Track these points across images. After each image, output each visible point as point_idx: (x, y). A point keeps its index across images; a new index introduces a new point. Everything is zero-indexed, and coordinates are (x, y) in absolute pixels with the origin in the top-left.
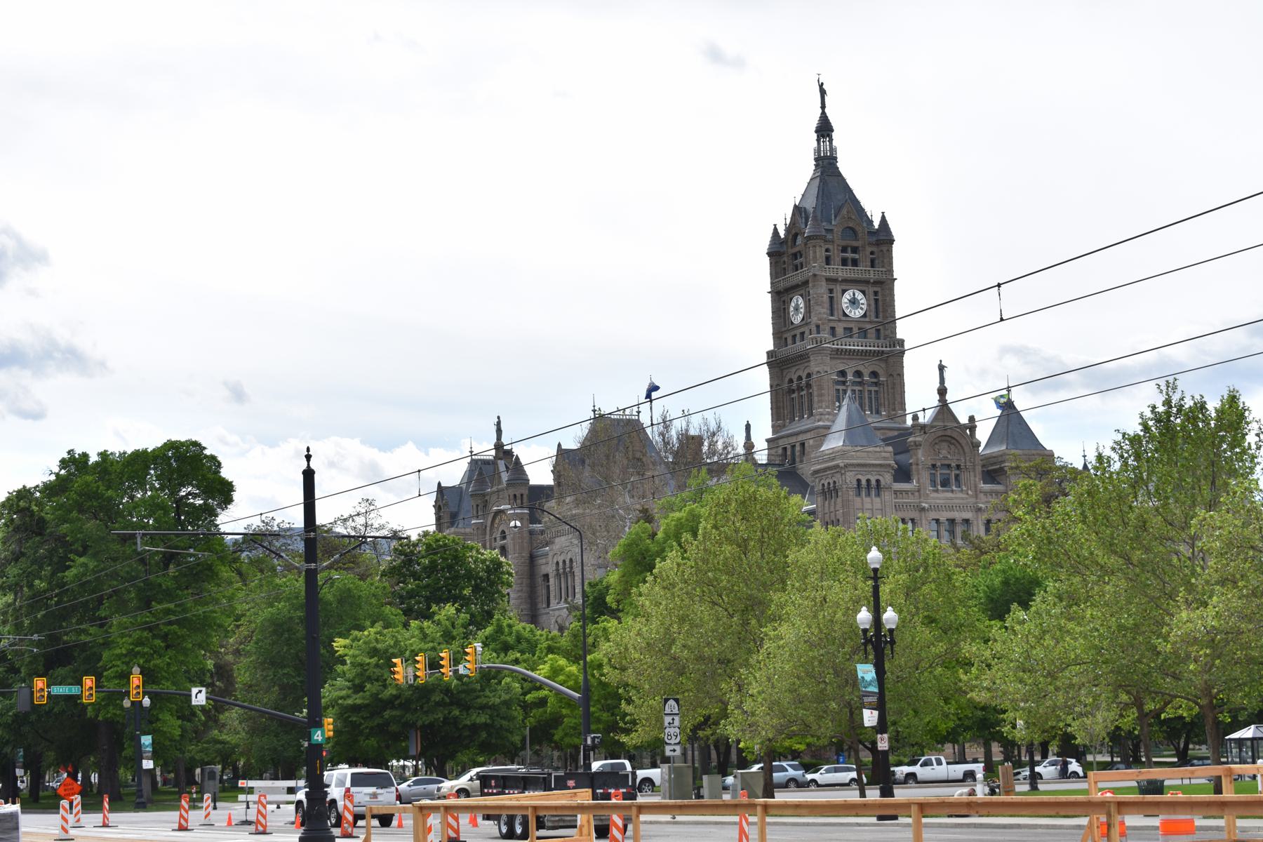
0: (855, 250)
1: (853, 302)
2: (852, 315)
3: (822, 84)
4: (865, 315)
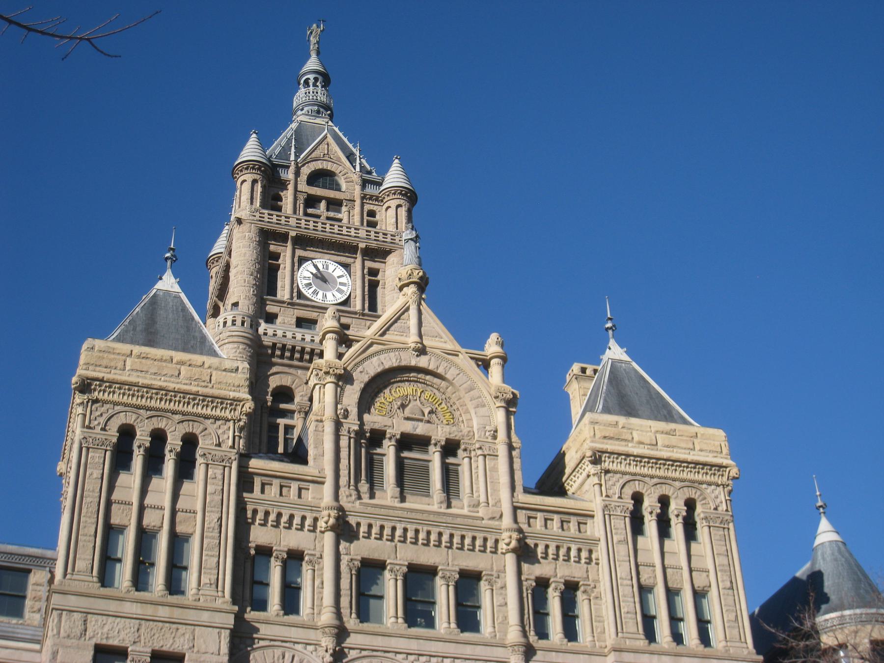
0: (334, 204)
4: (346, 302)
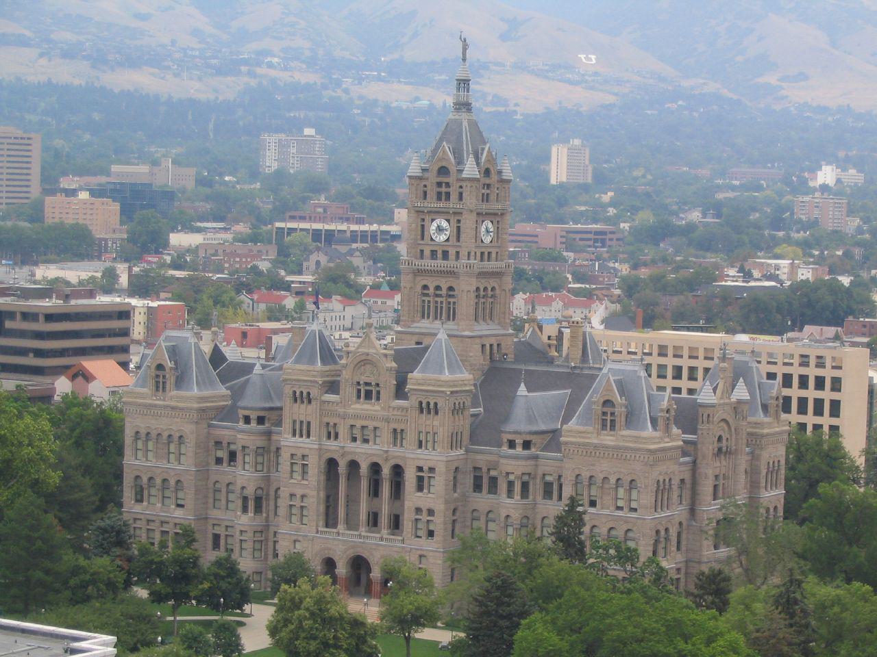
1: (440, 229)
2: (437, 240)
3: (465, 40)
4: (448, 240)
